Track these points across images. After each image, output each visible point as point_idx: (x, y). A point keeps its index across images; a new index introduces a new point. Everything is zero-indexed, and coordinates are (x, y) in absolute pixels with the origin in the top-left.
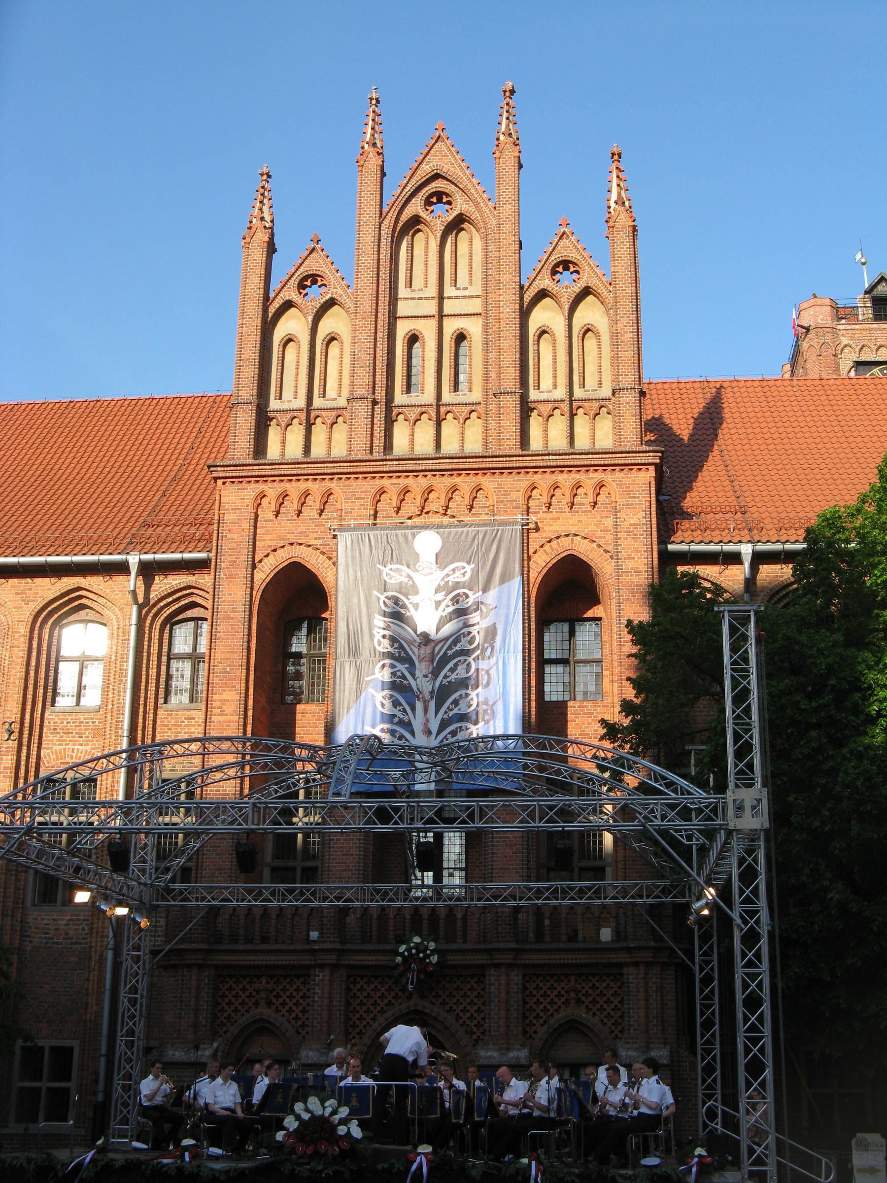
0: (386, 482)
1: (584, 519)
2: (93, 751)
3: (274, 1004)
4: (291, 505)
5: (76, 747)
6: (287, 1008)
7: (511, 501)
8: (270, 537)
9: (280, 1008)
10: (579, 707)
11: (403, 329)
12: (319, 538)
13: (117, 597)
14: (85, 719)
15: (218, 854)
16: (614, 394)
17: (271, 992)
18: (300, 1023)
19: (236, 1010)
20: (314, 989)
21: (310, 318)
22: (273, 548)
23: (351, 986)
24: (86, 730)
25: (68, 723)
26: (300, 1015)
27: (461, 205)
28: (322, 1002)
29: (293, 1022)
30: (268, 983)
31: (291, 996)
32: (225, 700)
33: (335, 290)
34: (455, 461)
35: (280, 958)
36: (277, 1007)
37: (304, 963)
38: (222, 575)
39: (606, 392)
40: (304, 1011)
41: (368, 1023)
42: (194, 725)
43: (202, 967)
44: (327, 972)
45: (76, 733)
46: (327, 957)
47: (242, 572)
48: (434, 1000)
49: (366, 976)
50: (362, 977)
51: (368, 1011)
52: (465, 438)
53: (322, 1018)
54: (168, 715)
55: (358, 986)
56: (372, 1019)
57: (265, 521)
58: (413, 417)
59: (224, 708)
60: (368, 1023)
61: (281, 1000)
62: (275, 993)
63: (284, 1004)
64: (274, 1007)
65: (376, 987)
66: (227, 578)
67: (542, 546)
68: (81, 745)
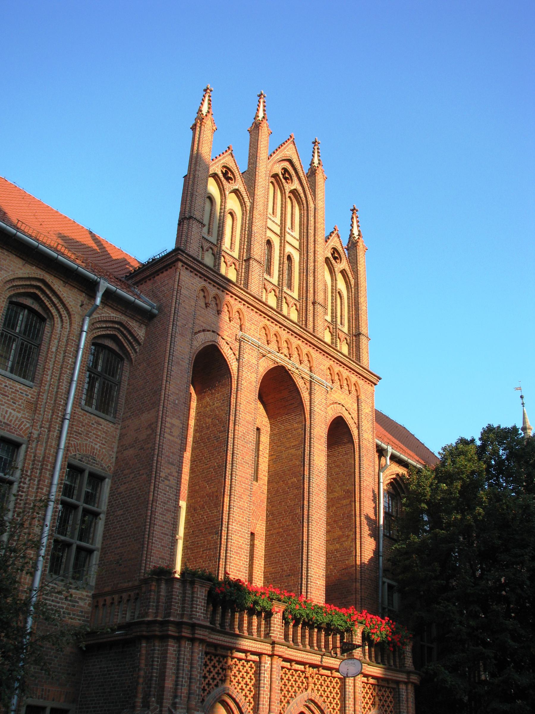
2: (23, 420)
5: (10, 410)
8: (202, 319)
13: (71, 303)
14: (20, 389)
15: (162, 546)
24: (20, 399)
25: (6, 386)
42: (100, 430)
45: (12, 398)
54: (84, 414)
68: (14, 410)
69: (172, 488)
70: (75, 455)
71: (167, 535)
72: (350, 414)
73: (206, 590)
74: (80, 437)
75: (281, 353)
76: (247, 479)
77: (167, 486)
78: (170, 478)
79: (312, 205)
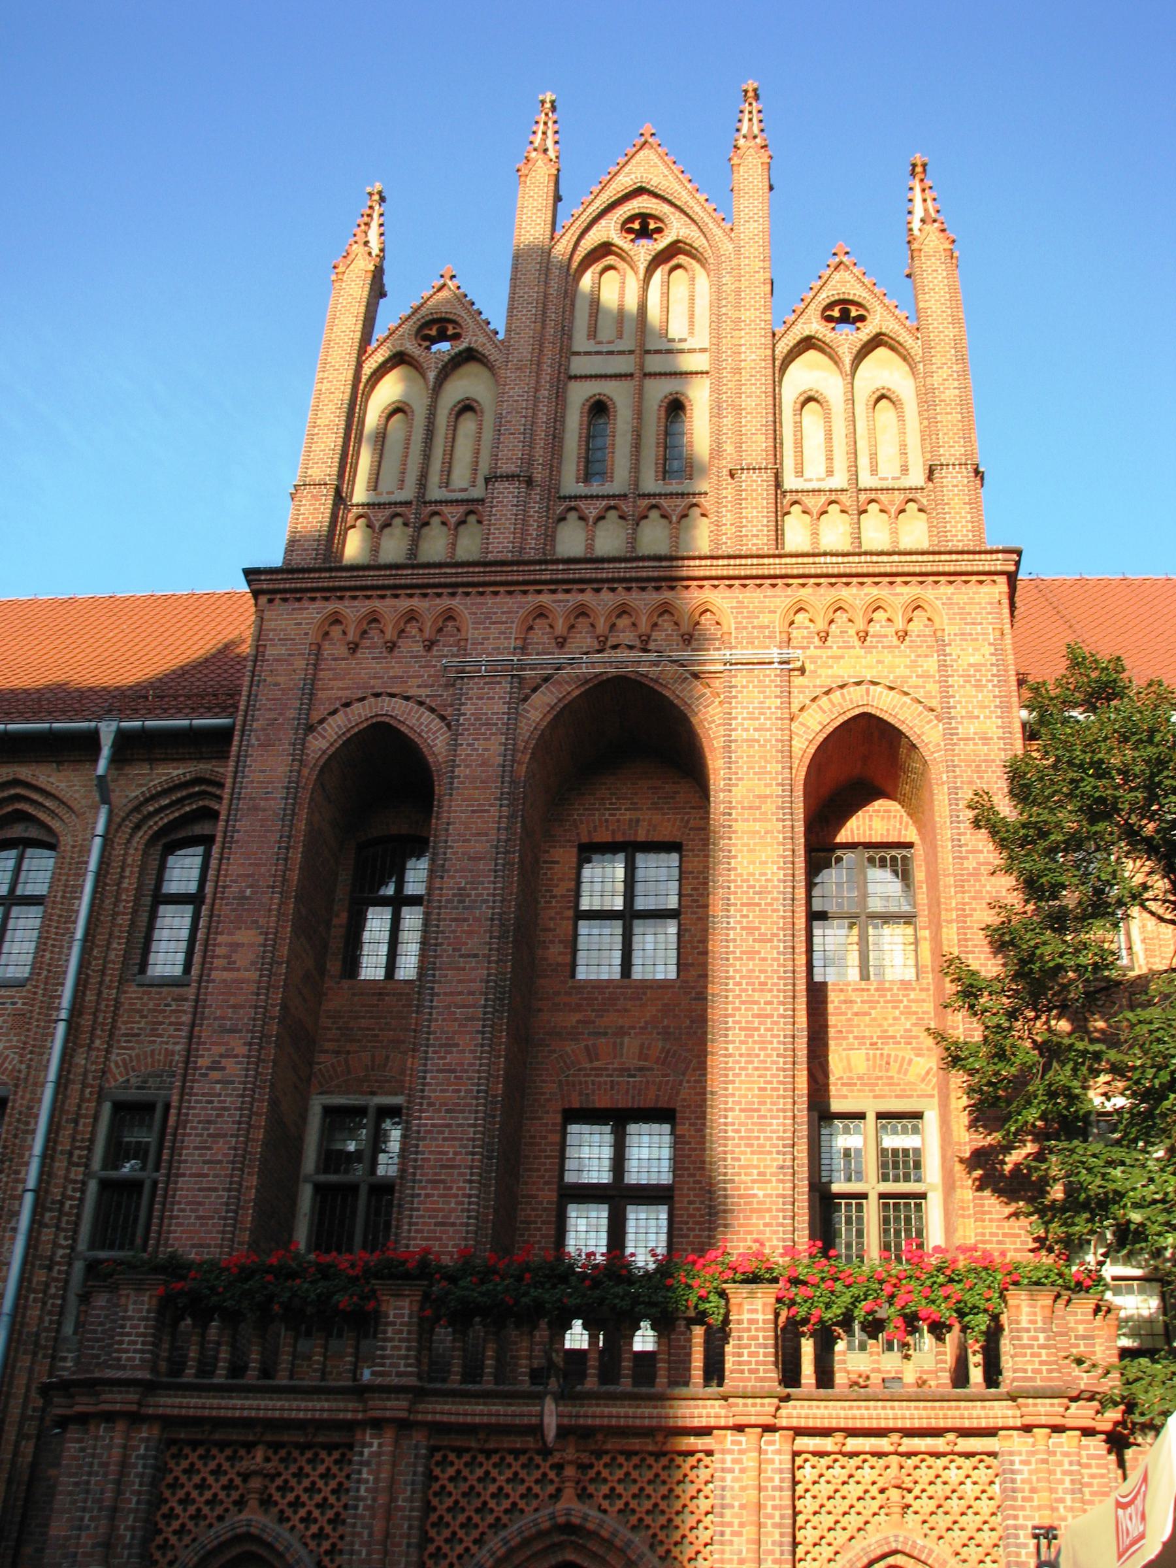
1: (888, 658)
2: (7, 1052)
3: (276, 1503)
6: (302, 1512)
8: (340, 684)
9: (289, 1512)
10: (877, 990)
11: (579, 394)
13: (77, 796)
15: (198, 1218)
16: (930, 478)
17: (272, 1477)
18: (326, 1545)
19: (197, 1516)
20: (360, 1472)
23: (437, 1471)
26: (328, 1529)
27: (676, 229)
28: (374, 1499)
29: (312, 1544)
30: (267, 1460)
31: (312, 1490)
32: (238, 945)
35: (295, 1404)
36: (282, 1512)
37: (341, 1416)
38: (254, 741)
39: (916, 477)
40: (336, 1521)
41: (467, 1549)
43: (135, 1419)
44: (389, 1436)
46: (389, 1404)
48: (605, 1504)
49: (468, 1450)
50: (460, 1452)
51: (468, 1524)
53: (371, 1535)
54: (144, 993)
55: (451, 1471)
56: (476, 1542)
57: (335, 660)
59: (234, 957)
60: (467, 1549)
61: (291, 1497)
62: (279, 1481)
63: (296, 1504)
64: (275, 1510)
65: (487, 1473)
67: (814, 700)
69: (233, 1082)
70: (128, 1081)
71: (216, 1190)
72: (906, 694)
73: (151, 1297)
74: (137, 1042)
75: (615, 647)
76: (471, 993)
77: (218, 1082)
78: (228, 1063)
79: (727, 247)
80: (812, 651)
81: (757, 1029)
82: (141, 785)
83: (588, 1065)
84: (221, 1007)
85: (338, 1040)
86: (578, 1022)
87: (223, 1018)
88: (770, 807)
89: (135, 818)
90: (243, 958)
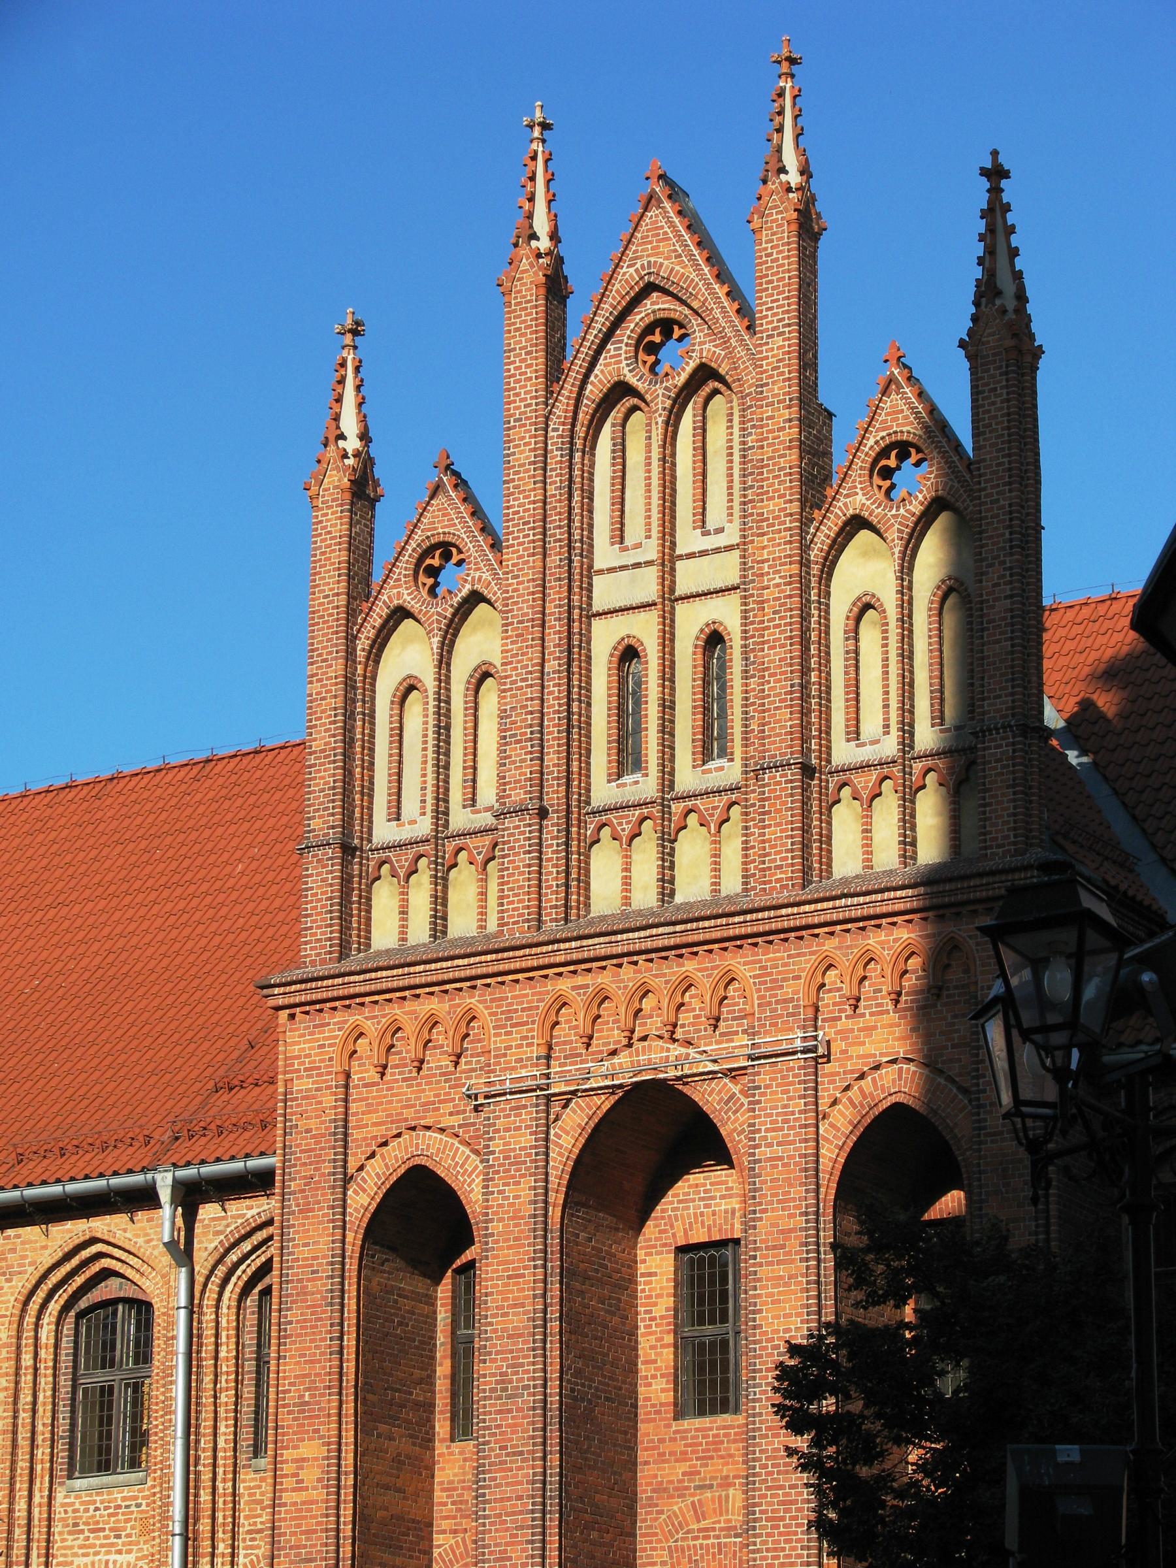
0: (564, 985)
4: (407, 1049)
5: (112, 1557)
7: (785, 1001)
8: (374, 1118)
11: (604, 639)
12: (458, 1113)
13: (156, 1253)
14: (124, 1499)
21: (436, 640)
22: (380, 1140)
24: (127, 1521)
25: (97, 1509)
27: (701, 347)
32: (304, 1460)
33: (477, 574)
34: (678, 928)
45: (111, 1529)
47: (327, 1197)
52: (706, 869)
57: (366, 1085)
58: (626, 829)
59: (303, 1474)
66: (300, 1211)
68: (119, 1552)
75: (644, 1038)
76: (520, 1498)
80: (843, 1023)
81: (783, 1519)
82: (221, 1232)
83: (695, 1527)
84: (294, 1534)
85: (455, 1517)
86: (684, 1474)
87: (298, 1547)
88: (794, 1244)
89: (221, 1271)
90: (310, 1475)
